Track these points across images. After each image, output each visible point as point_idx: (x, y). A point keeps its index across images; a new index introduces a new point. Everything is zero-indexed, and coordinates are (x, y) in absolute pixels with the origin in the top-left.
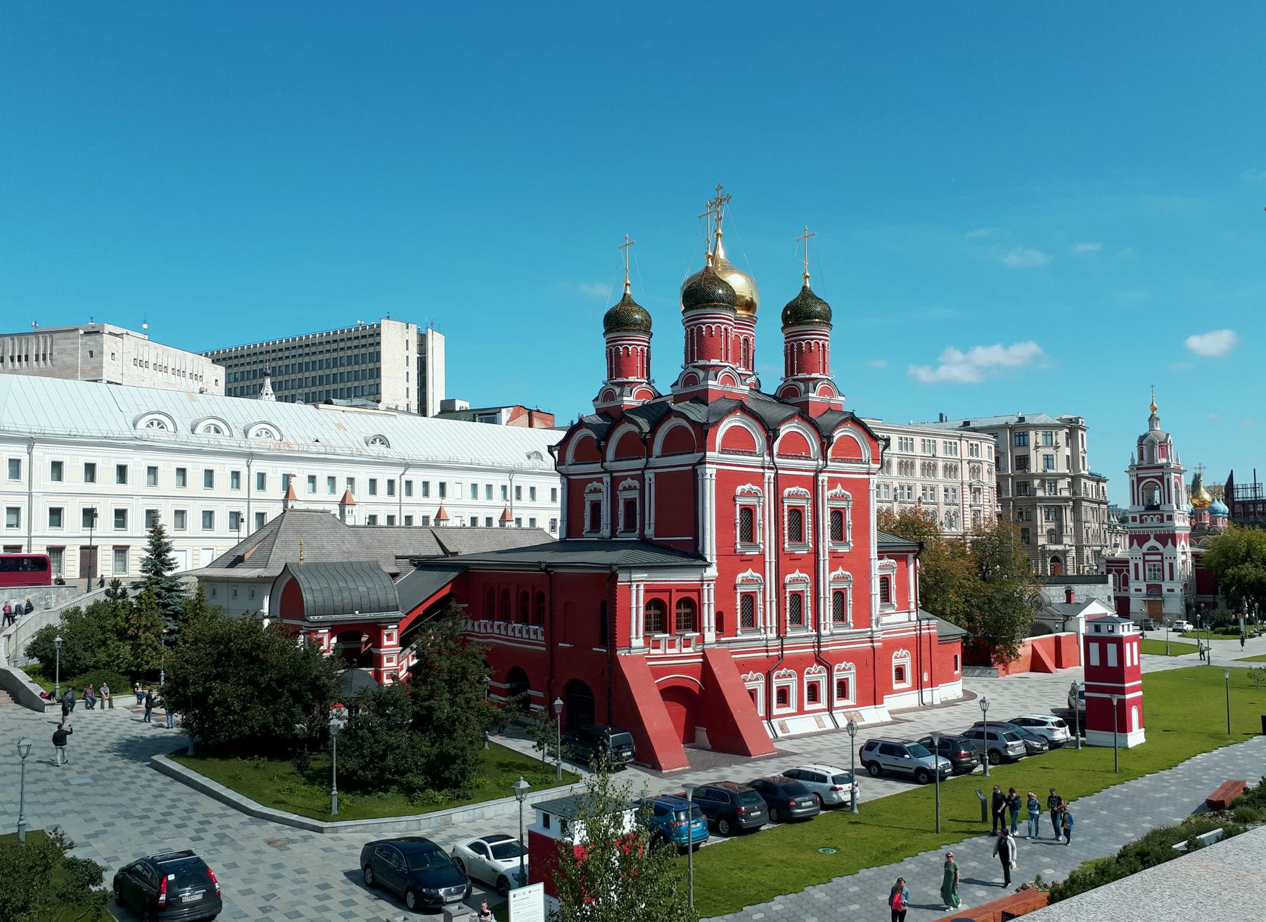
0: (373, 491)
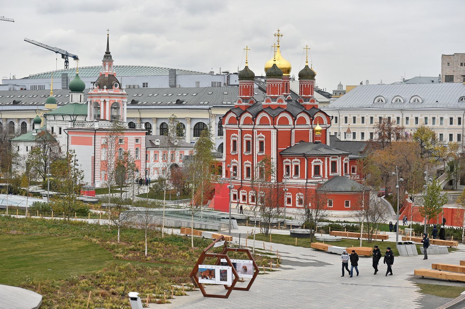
0: (451, 123)
